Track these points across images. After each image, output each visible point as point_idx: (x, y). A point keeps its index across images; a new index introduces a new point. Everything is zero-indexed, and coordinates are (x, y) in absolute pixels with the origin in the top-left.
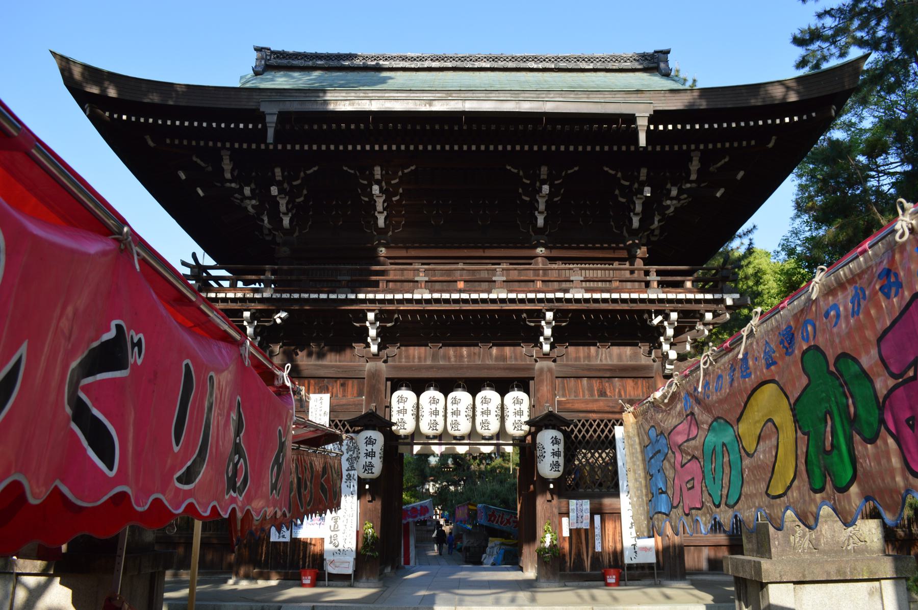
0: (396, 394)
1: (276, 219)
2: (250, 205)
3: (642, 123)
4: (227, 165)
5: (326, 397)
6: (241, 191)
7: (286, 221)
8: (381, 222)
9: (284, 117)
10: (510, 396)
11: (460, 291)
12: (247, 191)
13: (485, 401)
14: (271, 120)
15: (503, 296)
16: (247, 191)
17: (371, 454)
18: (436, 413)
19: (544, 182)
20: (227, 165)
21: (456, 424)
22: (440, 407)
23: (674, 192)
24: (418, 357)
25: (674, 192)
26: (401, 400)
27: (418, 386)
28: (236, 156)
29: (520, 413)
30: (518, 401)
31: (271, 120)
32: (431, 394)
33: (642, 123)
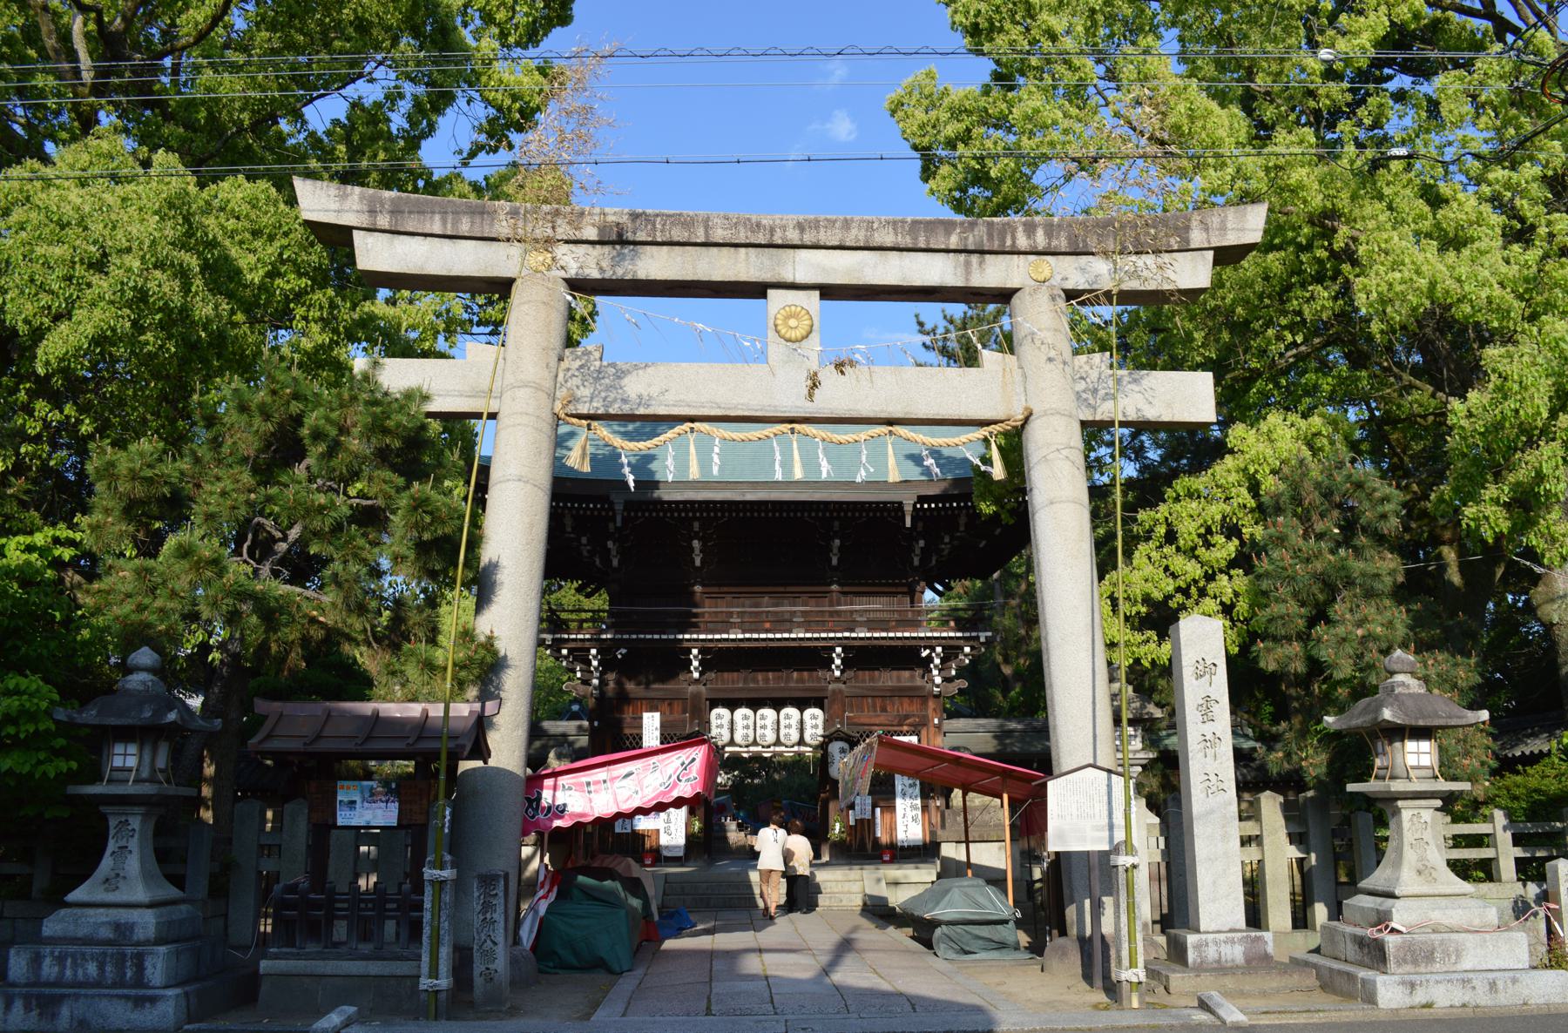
0: (715, 712)
1: (606, 560)
3: (908, 508)
5: (657, 715)
7: (615, 563)
8: (698, 563)
10: (809, 712)
11: (767, 631)
12: (584, 540)
13: (788, 717)
14: (619, 507)
15: (801, 635)
16: (584, 540)
18: (747, 727)
22: (751, 722)
23: (947, 540)
24: (734, 682)
25: (947, 540)
26: (719, 717)
27: (732, 705)
29: (816, 726)
30: (814, 717)
31: (619, 507)
32: (742, 712)
33: (908, 508)
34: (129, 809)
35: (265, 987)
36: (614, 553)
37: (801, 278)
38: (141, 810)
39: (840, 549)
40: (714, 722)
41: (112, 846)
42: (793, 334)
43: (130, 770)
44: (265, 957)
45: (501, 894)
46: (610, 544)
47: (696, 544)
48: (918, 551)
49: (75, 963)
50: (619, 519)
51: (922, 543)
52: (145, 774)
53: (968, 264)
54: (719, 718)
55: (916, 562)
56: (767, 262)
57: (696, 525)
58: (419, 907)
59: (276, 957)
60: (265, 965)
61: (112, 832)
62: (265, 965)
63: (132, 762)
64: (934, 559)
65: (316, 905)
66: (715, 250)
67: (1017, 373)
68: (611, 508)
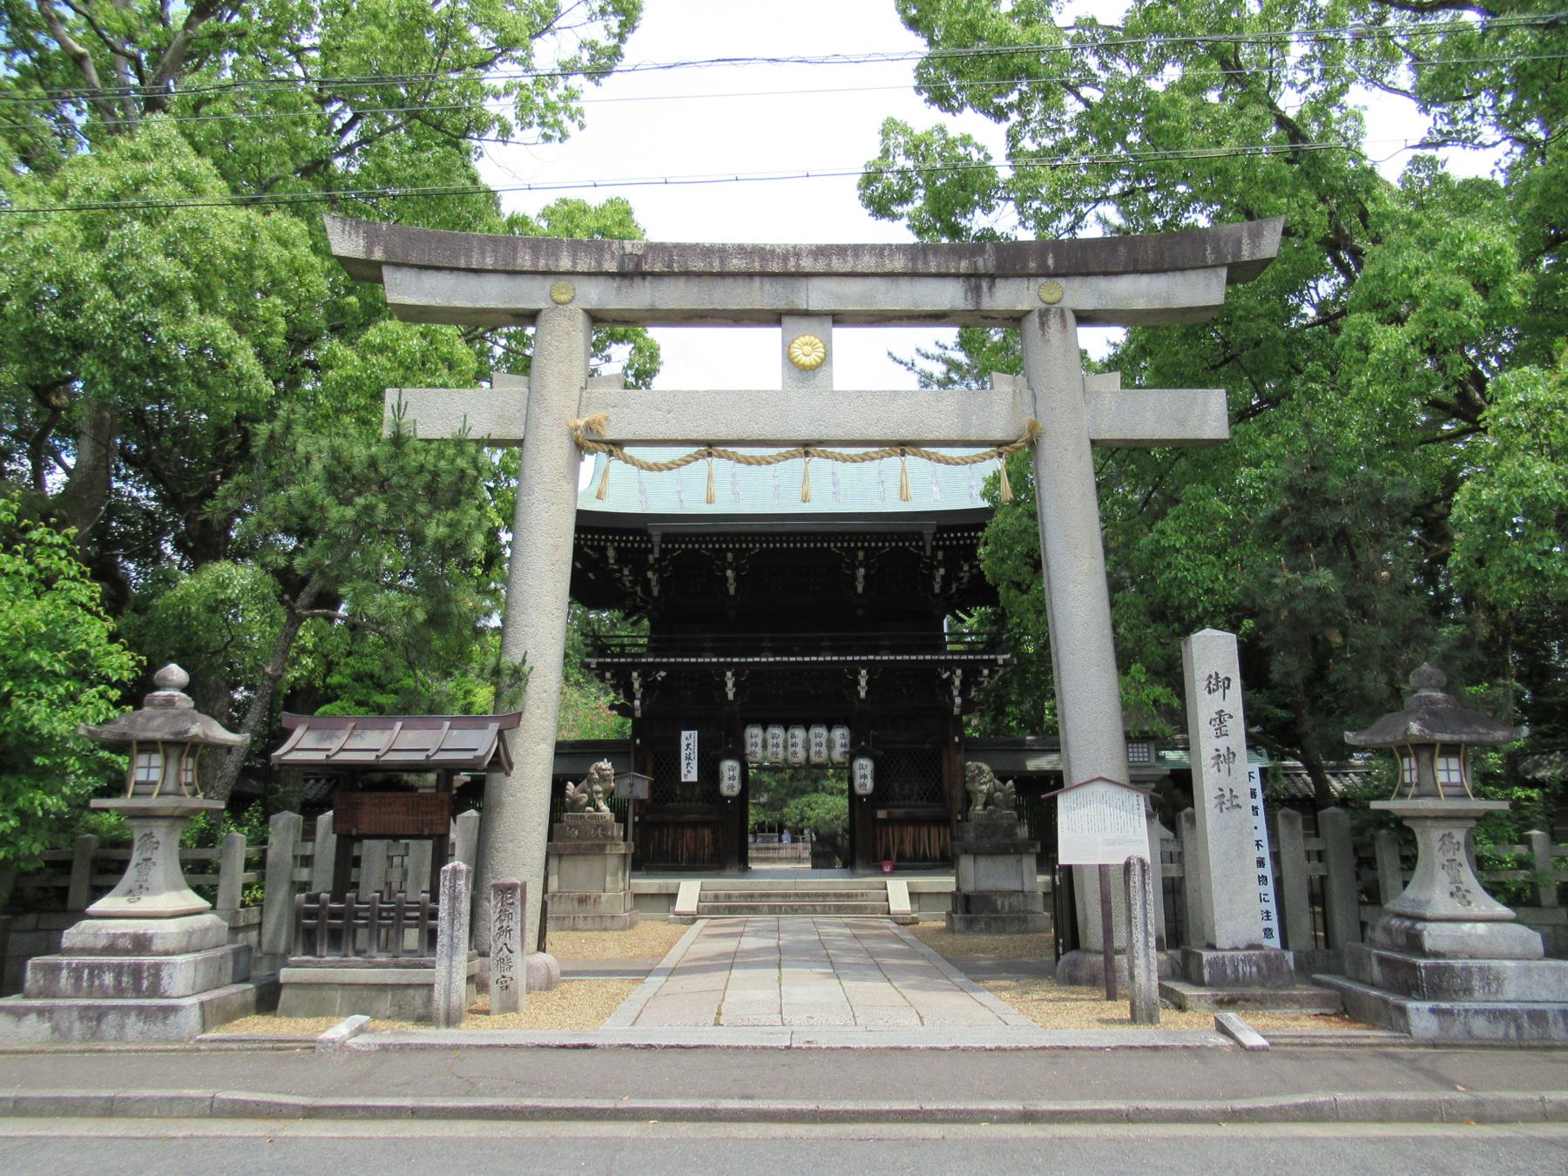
2: (627, 580)
4: (611, 553)
6: (620, 571)
7: (655, 592)
9: (666, 538)
12: (626, 572)
14: (657, 539)
16: (626, 572)
19: (861, 564)
20: (611, 553)
21: (795, 753)
23: (966, 568)
25: (966, 568)
28: (617, 549)
31: (657, 539)
33: (928, 538)
34: (153, 823)
35: (285, 995)
36: (653, 583)
37: (814, 305)
38: (165, 823)
39: (865, 577)
40: (749, 741)
41: (136, 857)
42: (807, 361)
43: (154, 783)
44: (287, 965)
45: (518, 903)
46: (650, 574)
47: (729, 573)
48: (938, 579)
49: (91, 974)
50: (656, 550)
51: (942, 571)
52: (170, 787)
53: (978, 289)
54: (754, 735)
55: (937, 589)
56: (781, 290)
57: (730, 556)
58: (434, 915)
59: (298, 965)
60: (285, 974)
61: (136, 845)
62: (285, 974)
63: (155, 775)
64: (954, 586)
65: (335, 915)
66: (730, 281)
67: (1027, 395)
68: (649, 540)
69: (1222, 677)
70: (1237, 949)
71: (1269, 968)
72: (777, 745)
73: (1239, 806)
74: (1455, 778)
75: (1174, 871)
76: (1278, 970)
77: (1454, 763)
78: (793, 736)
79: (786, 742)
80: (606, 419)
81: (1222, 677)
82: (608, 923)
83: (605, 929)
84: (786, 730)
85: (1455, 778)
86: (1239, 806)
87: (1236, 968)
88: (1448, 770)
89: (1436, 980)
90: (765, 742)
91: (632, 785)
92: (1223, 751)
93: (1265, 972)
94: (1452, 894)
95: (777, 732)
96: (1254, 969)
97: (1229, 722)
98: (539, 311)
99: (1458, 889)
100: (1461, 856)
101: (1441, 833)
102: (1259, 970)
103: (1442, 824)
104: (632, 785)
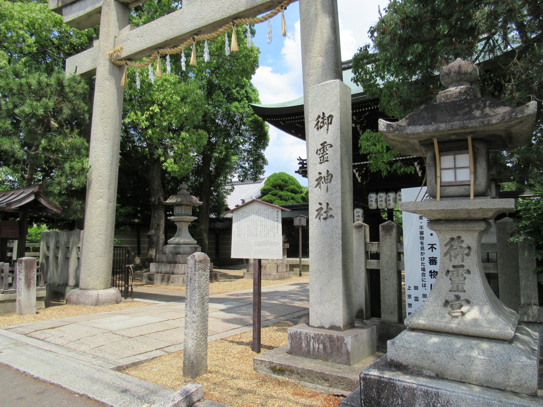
17: (359, 216)
21: (390, 204)
40: (370, 199)
54: (372, 197)
69: (327, 115)
70: (322, 327)
71: (332, 348)
72: (382, 201)
73: (331, 216)
74: (464, 175)
75: (373, 264)
76: (339, 349)
77: (464, 160)
78: (389, 196)
79: (386, 199)
80: (122, 49)
81: (327, 115)
82: (268, 277)
83: (267, 279)
84: (387, 194)
85: (464, 175)
86: (331, 216)
87: (308, 343)
88: (455, 168)
89: (374, 394)
90: (377, 199)
91: (300, 220)
92: (324, 174)
93: (329, 350)
94: (446, 303)
95: (382, 195)
96: (321, 346)
97: (329, 151)
98: (100, 8)
99: (458, 298)
100: (473, 262)
101: (448, 237)
102: (325, 348)
103: (451, 226)
104: (300, 220)
